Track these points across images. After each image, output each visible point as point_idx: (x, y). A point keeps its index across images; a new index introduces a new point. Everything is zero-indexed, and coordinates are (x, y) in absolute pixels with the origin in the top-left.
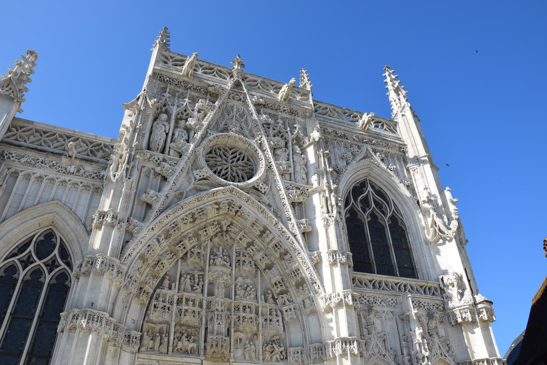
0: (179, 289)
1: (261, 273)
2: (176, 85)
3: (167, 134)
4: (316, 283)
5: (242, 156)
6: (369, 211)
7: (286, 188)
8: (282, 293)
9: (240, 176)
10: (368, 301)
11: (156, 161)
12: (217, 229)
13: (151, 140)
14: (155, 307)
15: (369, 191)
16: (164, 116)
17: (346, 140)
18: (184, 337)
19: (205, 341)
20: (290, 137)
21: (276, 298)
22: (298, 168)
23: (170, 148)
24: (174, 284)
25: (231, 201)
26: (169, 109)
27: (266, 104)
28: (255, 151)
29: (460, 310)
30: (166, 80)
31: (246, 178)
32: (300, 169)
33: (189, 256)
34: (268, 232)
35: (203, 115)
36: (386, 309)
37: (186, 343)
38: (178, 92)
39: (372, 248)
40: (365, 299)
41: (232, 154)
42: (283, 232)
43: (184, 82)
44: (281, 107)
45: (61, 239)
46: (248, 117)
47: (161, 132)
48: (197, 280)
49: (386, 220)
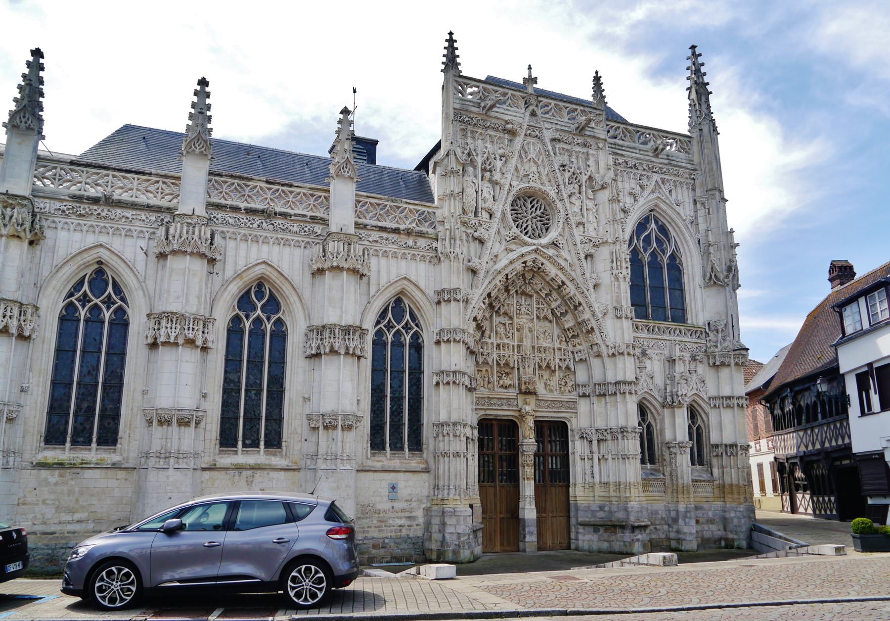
3: (476, 192)
5: (539, 204)
6: (649, 252)
9: (539, 228)
16: (470, 169)
17: (636, 171)
22: (591, 219)
30: (465, 120)
31: (544, 231)
34: (565, 286)
36: (656, 352)
41: (531, 203)
49: (665, 260)
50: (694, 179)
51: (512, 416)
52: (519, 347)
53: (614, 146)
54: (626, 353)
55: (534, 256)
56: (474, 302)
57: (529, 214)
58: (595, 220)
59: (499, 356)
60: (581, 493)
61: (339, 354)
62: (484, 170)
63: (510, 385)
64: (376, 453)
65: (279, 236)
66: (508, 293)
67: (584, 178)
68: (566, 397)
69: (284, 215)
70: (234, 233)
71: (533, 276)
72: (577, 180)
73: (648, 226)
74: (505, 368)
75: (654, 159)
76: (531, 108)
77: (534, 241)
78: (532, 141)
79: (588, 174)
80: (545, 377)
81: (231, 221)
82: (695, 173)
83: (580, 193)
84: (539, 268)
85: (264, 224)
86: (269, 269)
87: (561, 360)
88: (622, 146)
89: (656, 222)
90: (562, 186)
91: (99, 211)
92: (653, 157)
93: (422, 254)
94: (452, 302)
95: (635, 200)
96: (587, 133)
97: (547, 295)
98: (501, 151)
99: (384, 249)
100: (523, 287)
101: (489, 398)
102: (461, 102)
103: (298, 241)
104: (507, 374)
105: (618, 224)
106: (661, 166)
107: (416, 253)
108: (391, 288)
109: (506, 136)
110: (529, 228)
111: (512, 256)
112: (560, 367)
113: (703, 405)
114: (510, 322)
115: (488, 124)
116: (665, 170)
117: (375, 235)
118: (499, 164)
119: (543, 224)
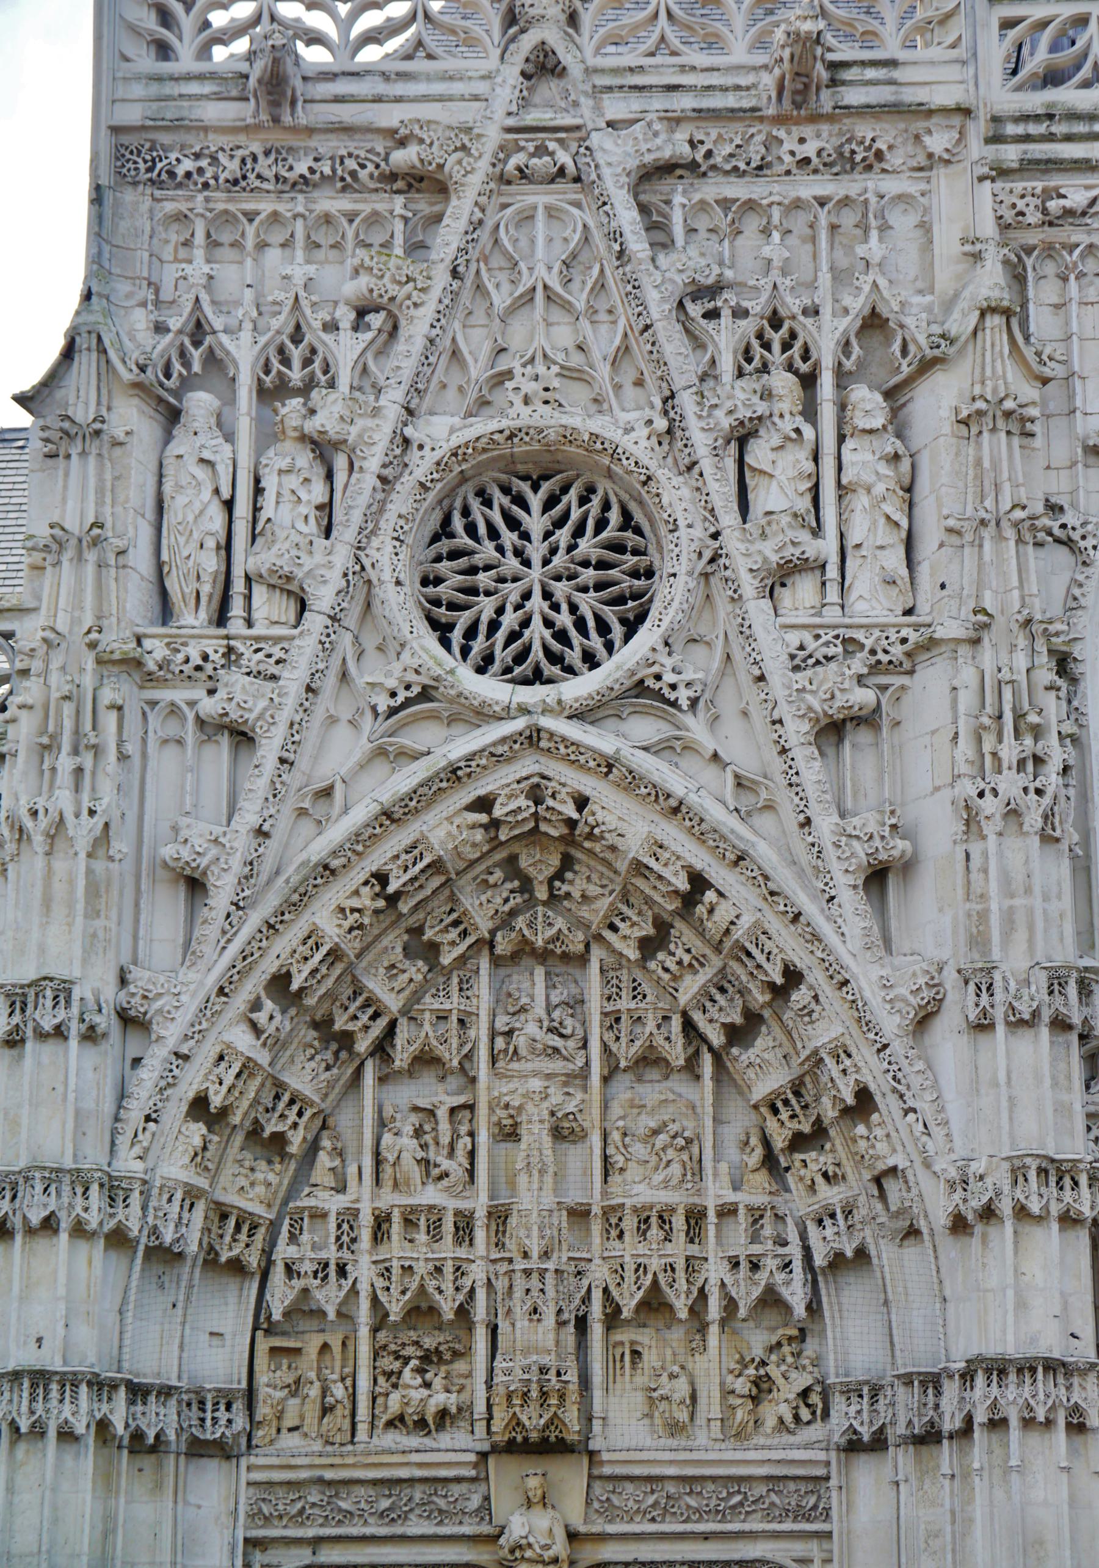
0: (378, 1181)
1: (717, 1056)
2: (236, 182)
3: (229, 505)
4: (914, 1110)
7: (793, 657)
8: (798, 1142)
9: (591, 623)
11: (198, 668)
12: (506, 900)
13: (165, 557)
14: (289, 1269)
18: (407, 1373)
19: (489, 1386)
21: (784, 1164)
23: (248, 579)
24: (352, 1170)
25: (535, 780)
26: (219, 354)
27: (699, 157)
28: (645, 483)
30: (180, 171)
32: (873, 528)
33: (400, 1040)
34: (710, 896)
35: (384, 336)
38: (251, 216)
41: (550, 503)
42: (772, 893)
43: (267, 153)
44: (787, 146)
46: (608, 272)
47: (197, 506)
48: (445, 1140)
52: (499, 1216)
53: (1034, 129)
54: (1006, 1207)
55: (528, 765)
56: (171, 1033)
58: (884, 535)
59: (386, 1273)
63: (443, 1414)
66: (433, 965)
71: (567, 862)
72: (796, 350)
76: (528, 42)
78: (538, 197)
79: (857, 304)
80: (650, 1358)
83: (810, 412)
84: (571, 824)
87: (735, 1265)
90: (687, 401)
94: (29, 1045)
96: (854, 97)
97: (649, 947)
98: (355, 288)
100: (520, 922)
101: (320, 1481)
102: (154, 89)
104: (431, 1358)
105: (1000, 538)
110: (537, 632)
112: (730, 1305)
114: (461, 1100)
115: (302, 168)
119: (620, 600)
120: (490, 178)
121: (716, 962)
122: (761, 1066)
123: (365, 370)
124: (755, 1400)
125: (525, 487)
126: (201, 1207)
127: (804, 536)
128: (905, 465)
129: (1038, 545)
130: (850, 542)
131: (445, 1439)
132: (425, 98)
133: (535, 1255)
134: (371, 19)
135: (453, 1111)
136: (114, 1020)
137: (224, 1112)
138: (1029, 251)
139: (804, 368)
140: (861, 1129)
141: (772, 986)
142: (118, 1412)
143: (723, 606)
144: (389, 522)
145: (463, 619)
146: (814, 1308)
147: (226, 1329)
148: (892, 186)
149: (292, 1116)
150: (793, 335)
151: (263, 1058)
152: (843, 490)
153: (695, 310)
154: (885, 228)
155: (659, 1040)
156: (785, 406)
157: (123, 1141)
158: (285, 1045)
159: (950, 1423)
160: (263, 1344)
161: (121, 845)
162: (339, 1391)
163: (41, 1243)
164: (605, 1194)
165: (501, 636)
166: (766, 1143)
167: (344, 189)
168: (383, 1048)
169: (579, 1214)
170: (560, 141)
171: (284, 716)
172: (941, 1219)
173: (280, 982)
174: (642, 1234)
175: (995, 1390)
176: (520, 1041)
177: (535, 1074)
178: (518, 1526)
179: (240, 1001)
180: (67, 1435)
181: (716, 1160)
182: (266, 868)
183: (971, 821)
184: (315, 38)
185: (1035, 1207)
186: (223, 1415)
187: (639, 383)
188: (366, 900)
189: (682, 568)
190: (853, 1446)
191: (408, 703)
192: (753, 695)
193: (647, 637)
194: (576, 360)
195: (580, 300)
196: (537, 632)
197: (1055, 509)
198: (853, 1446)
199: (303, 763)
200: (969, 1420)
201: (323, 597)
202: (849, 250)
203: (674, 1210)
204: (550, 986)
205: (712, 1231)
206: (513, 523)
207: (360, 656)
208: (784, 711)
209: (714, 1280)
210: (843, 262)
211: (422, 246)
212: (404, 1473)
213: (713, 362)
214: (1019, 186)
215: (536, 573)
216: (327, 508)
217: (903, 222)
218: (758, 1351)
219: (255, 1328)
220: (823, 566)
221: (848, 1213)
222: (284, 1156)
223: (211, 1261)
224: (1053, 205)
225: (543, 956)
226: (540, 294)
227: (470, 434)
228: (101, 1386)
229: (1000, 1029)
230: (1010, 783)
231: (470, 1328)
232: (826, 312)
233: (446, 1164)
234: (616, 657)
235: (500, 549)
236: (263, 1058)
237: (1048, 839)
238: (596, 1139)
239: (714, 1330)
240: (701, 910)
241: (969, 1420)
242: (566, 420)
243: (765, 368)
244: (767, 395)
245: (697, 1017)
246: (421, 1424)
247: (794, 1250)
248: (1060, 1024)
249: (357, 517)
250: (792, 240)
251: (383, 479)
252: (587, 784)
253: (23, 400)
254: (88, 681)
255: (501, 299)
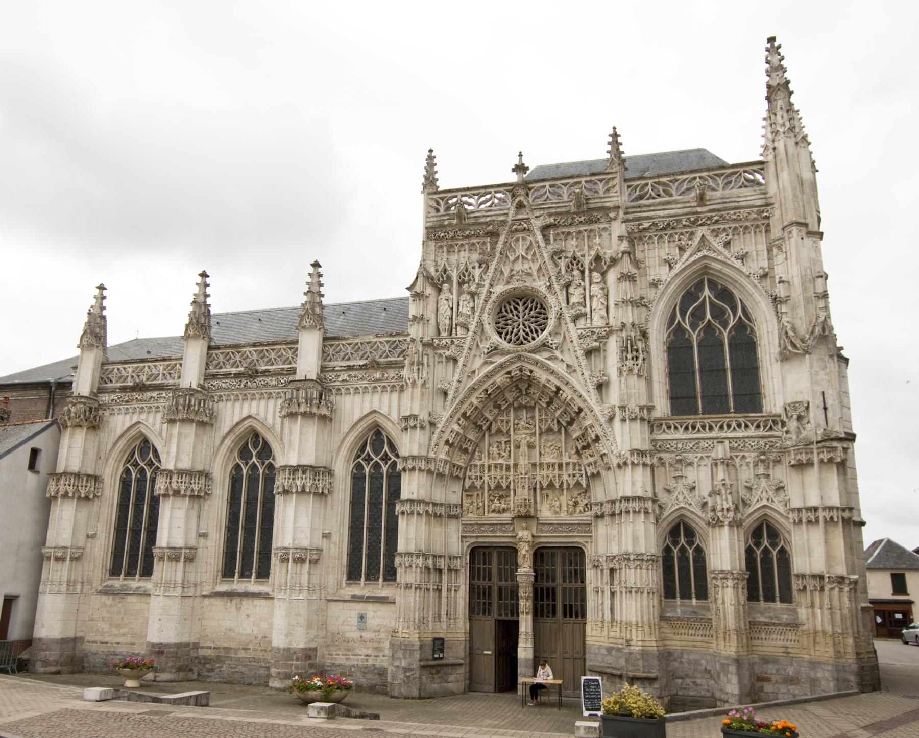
0: (489, 458)
1: (565, 428)
8: (584, 448)
10: (676, 448)
15: (705, 297)
16: (446, 286)
17: (672, 232)
18: (496, 501)
20: (586, 262)
23: (456, 325)
29: (794, 450)
31: (540, 331)
32: (598, 305)
34: (561, 392)
36: (700, 455)
37: (498, 505)
38: (457, 245)
39: (698, 378)
40: (672, 447)
41: (524, 304)
45: (387, 437)
49: (726, 334)
50: (767, 218)
51: (510, 542)
52: (516, 465)
54: (629, 462)
56: (440, 426)
57: (520, 319)
58: (600, 307)
59: (491, 478)
60: (597, 633)
61: (292, 493)
62: (461, 284)
63: (504, 510)
64: (351, 584)
65: (263, 391)
66: (500, 410)
67: (586, 262)
68: (576, 518)
69: (265, 373)
70: (229, 395)
72: (579, 265)
73: (700, 294)
74: (501, 491)
75: (699, 209)
76: (517, 200)
77: (519, 348)
78: (520, 235)
79: (593, 253)
80: (551, 497)
81: (224, 385)
82: (769, 208)
83: (583, 280)
84: (529, 377)
85: (249, 383)
86: (255, 422)
88: (650, 206)
89: (712, 285)
90: (553, 278)
91: (137, 396)
92: (698, 206)
93: (392, 384)
95: (671, 267)
99: (355, 386)
100: (519, 399)
101: (477, 524)
103: (279, 393)
104: (501, 497)
106: (709, 215)
107: (386, 384)
108: (362, 423)
109: (489, 239)
110: (521, 333)
111: (491, 367)
112: (569, 485)
113: (782, 520)
114: (507, 440)
115: (467, 233)
116: (716, 218)
117: (344, 376)
118: (477, 272)
120: (509, 231)
121: (564, 407)
122: (575, 431)
123: (482, 277)
124: (575, 506)
125: (518, 301)
126: (448, 464)
127: (581, 308)
128: (606, 290)
129: (638, 307)
130: (593, 308)
131: (504, 515)
132: (494, 215)
133: (523, 473)
134: (483, 199)
135: (505, 442)
136: (427, 423)
137: (453, 443)
138: (635, 238)
139: (581, 269)
140: (597, 444)
141: (575, 412)
142: (430, 509)
143: (563, 325)
144: (486, 310)
145: (505, 331)
146: (588, 485)
147: (456, 490)
148: (602, 226)
149: (469, 444)
150: (579, 262)
151: (461, 431)
152: (591, 297)
153: (556, 258)
154: (600, 236)
155: (552, 425)
156: (577, 278)
157: (430, 450)
158: (467, 428)
159: (617, 512)
160: (464, 494)
161: (429, 385)
162: (481, 504)
163: (412, 473)
164: (540, 460)
165: (513, 334)
166: (577, 448)
167: (477, 237)
168: (489, 428)
169: (534, 465)
170: (525, 222)
171: (464, 355)
172: (615, 465)
173: (464, 414)
174: (548, 469)
175: (626, 504)
176: (520, 426)
177: (524, 433)
178: (520, 534)
179: (455, 419)
180: (418, 514)
181: (566, 452)
182: (461, 389)
183: (621, 373)
184: (470, 204)
185: (636, 462)
186: (455, 509)
187: (544, 275)
188: (483, 396)
189: (553, 317)
190: (597, 517)
191: (491, 351)
192: (570, 345)
193: (546, 332)
194: (529, 271)
195: (529, 257)
196: (521, 333)
197: (642, 298)
198: (597, 517)
199: (469, 365)
200: (621, 511)
201: (472, 328)
202: (592, 241)
203: (555, 464)
204: (527, 414)
205: (564, 468)
206: (516, 309)
207: (481, 341)
208: (577, 348)
209: (565, 479)
210: (591, 244)
211: (495, 248)
212: (495, 522)
213: (560, 269)
214: (632, 223)
215: (521, 320)
216: (473, 308)
217: (605, 234)
218: (576, 495)
219: (463, 490)
220: (586, 315)
221: (595, 463)
222: (468, 453)
223: (452, 476)
224: (640, 227)
225: (525, 407)
226: (520, 257)
227: (505, 289)
228: (426, 503)
229: (628, 420)
230: (630, 363)
231: (510, 490)
232: (586, 256)
233: (504, 454)
234: (540, 337)
235: (513, 315)
236: (461, 431)
237: (639, 376)
238: (537, 448)
239: (565, 490)
240: (559, 395)
241: (621, 511)
242: (526, 284)
243: (572, 270)
244: (573, 276)
245: (560, 420)
246: (499, 512)
247: (583, 472)
248: (642, 419)
249: (479, 309)
250: (579, 240)
251: (486, 301)
252: (532, 367)
253: (408, 288)
254: (420, 349)
255: (512, 259)
